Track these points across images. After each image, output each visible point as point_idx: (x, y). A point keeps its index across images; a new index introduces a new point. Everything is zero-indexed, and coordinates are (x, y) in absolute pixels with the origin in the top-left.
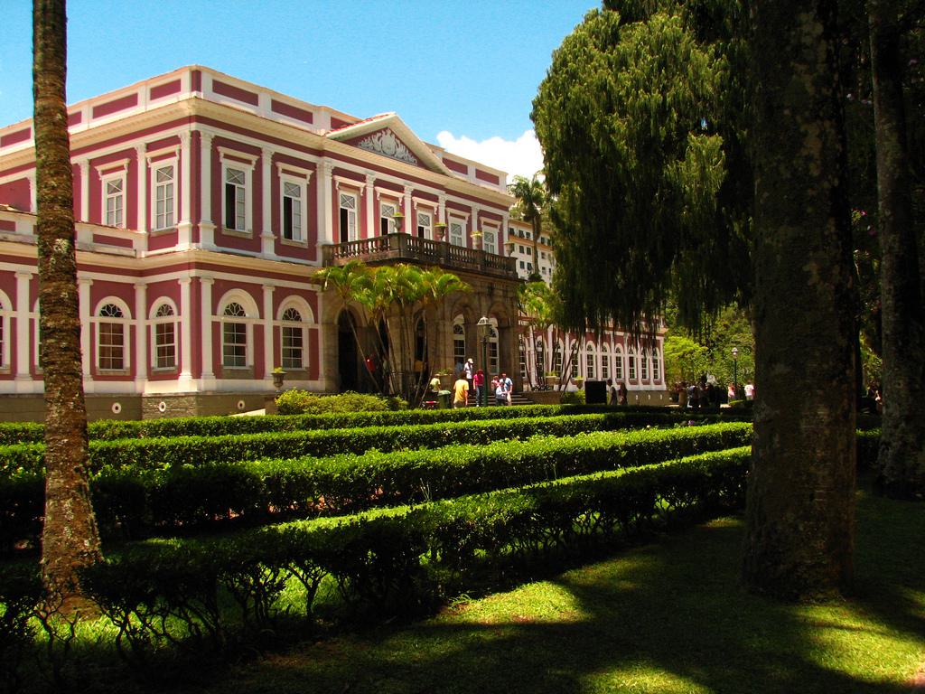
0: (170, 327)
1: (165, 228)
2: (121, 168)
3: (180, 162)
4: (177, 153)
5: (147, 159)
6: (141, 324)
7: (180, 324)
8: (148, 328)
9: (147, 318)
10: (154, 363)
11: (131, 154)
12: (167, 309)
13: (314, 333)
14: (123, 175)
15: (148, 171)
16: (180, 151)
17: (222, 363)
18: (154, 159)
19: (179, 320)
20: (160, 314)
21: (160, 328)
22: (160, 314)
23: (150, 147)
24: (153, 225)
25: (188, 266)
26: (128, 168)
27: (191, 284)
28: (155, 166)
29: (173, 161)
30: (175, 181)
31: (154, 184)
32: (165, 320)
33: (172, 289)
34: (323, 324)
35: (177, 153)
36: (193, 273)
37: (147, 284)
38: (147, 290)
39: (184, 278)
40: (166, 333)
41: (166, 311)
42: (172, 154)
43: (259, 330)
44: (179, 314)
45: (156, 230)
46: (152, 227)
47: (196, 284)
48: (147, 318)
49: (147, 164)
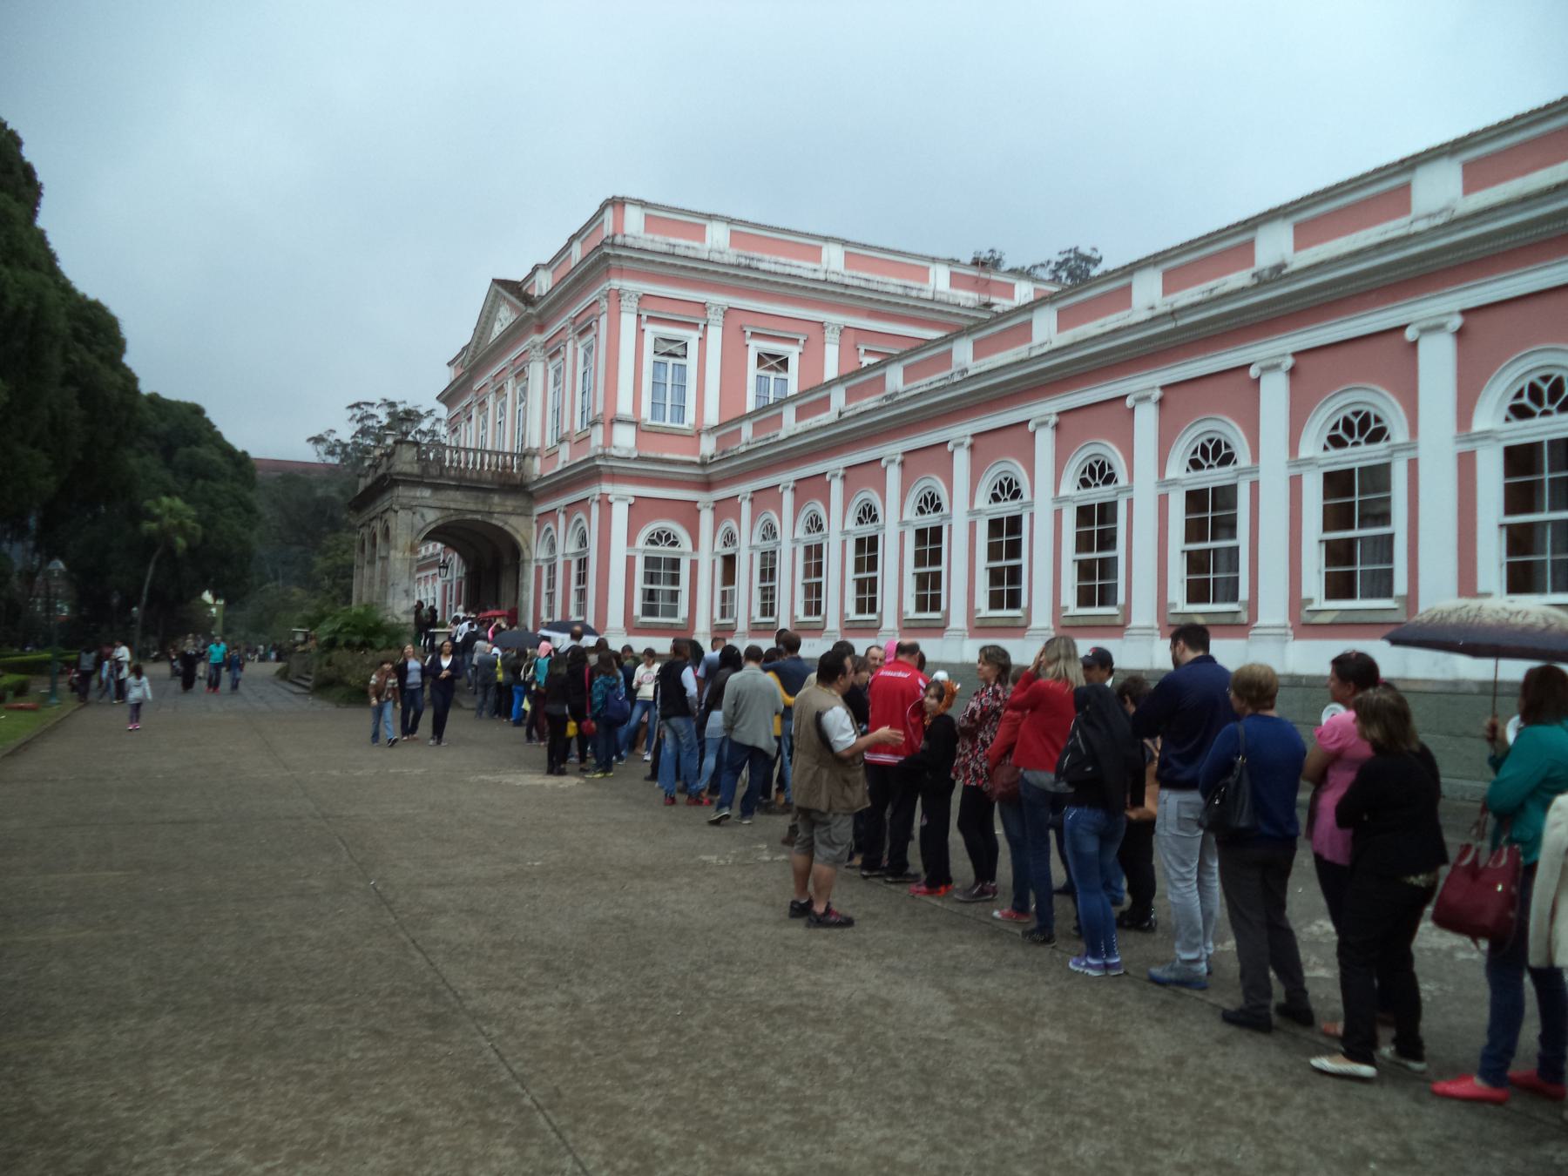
1: (668, 423)
4: (701, 327)
5: (639, 316)
7: (694, 565)
8: (630, 561)
9: (631, 540)
10: (637, 609)
15: (640, 332)
16: (706, 326)
18: (651, 319)
19: (694, 558)
21: (651, 562)
23: (644, 298)
28: (652, 330)
29: (692, 337)
32: (663, 550)
35: (701, 327)
42: (696, 325)
44: (695, 546)
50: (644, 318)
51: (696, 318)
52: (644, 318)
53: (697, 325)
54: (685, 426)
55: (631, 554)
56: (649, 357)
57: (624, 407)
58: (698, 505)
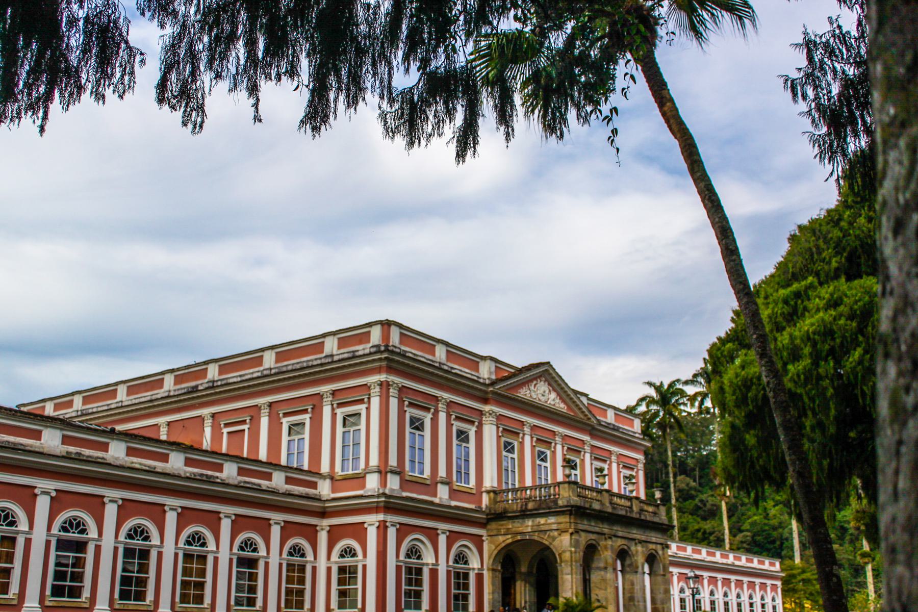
0: (353, 570)
1: (351, 472)
2: (305, 411)
3: (368, 409)
4: (366, 400)
5: (332, 405)
6: (274, 561)
7: (364, 567)
8: (329, 570)
9: (329, 558)
11: (316, 402)
12: (350, 551)
13: (480, 577)
14: (306, 418)
15: (334, 415)
16: (369, 399)
17: (403, 607)
18: (340, 405)
19: (364, 563)
20: (342, 556)
21: (342, 570)
22: (342, 556)
23: (334, 393)
24: (338, 468)
25: (375, 509)
26: (312, 412)
27: (378, 527)
28: (341, 412)
29: (362, 408)
30: (363, 426)
31: (340, 429)
32: (348, 561)
33: (359, 532)
34: (488, 570)
35: (366, 400)
36: (381, 517)
37: (330, 526)
38: (329, 532)
39: (372, 520)
40: (347, 574)
41: (349, 552)
42: (361, 401)
43: (434, 573)
44: (365, 555)
45: (340, 473)
46: (336, 470)
47: (382, 528)
48: (329, 558)
49: (333, 409)
50: (335, 406)
51: (361, 396)
52: (335, 406)
53: (363, 400)
54: (360, 471)
55: (329, 565)
56: (340, 429)
57: (325, 468)
58: (366, 525)
